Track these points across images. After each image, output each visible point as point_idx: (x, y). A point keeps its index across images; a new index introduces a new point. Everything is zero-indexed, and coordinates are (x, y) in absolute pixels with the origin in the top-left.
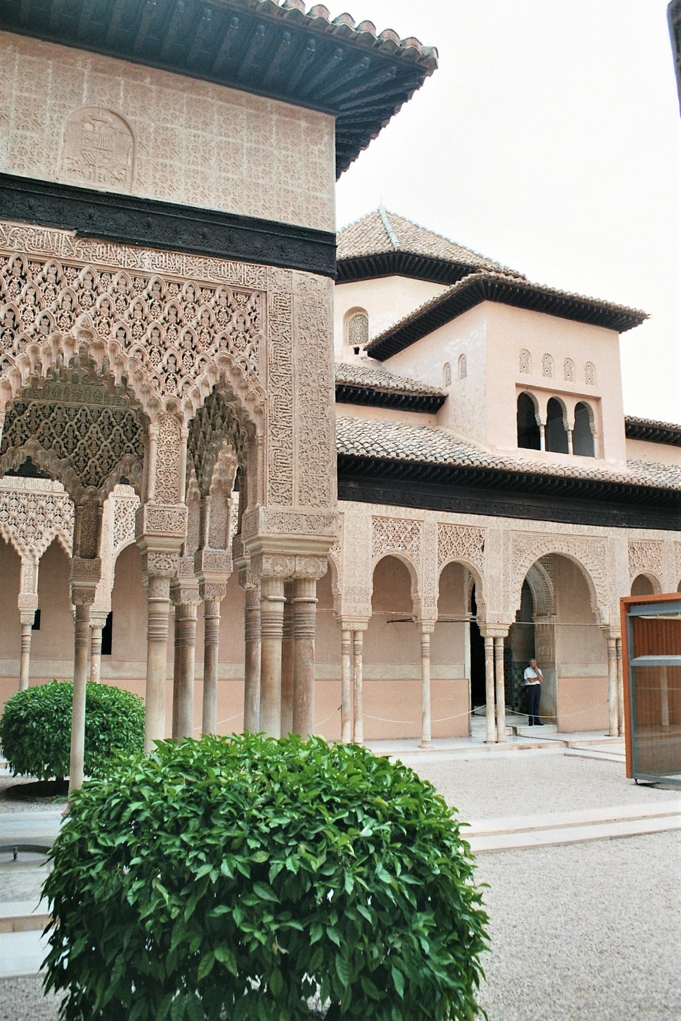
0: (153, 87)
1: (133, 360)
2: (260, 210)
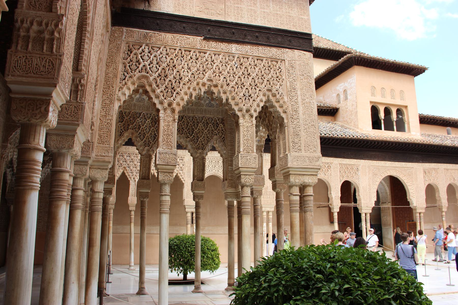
1: (231, 92)
2: (279, 25)
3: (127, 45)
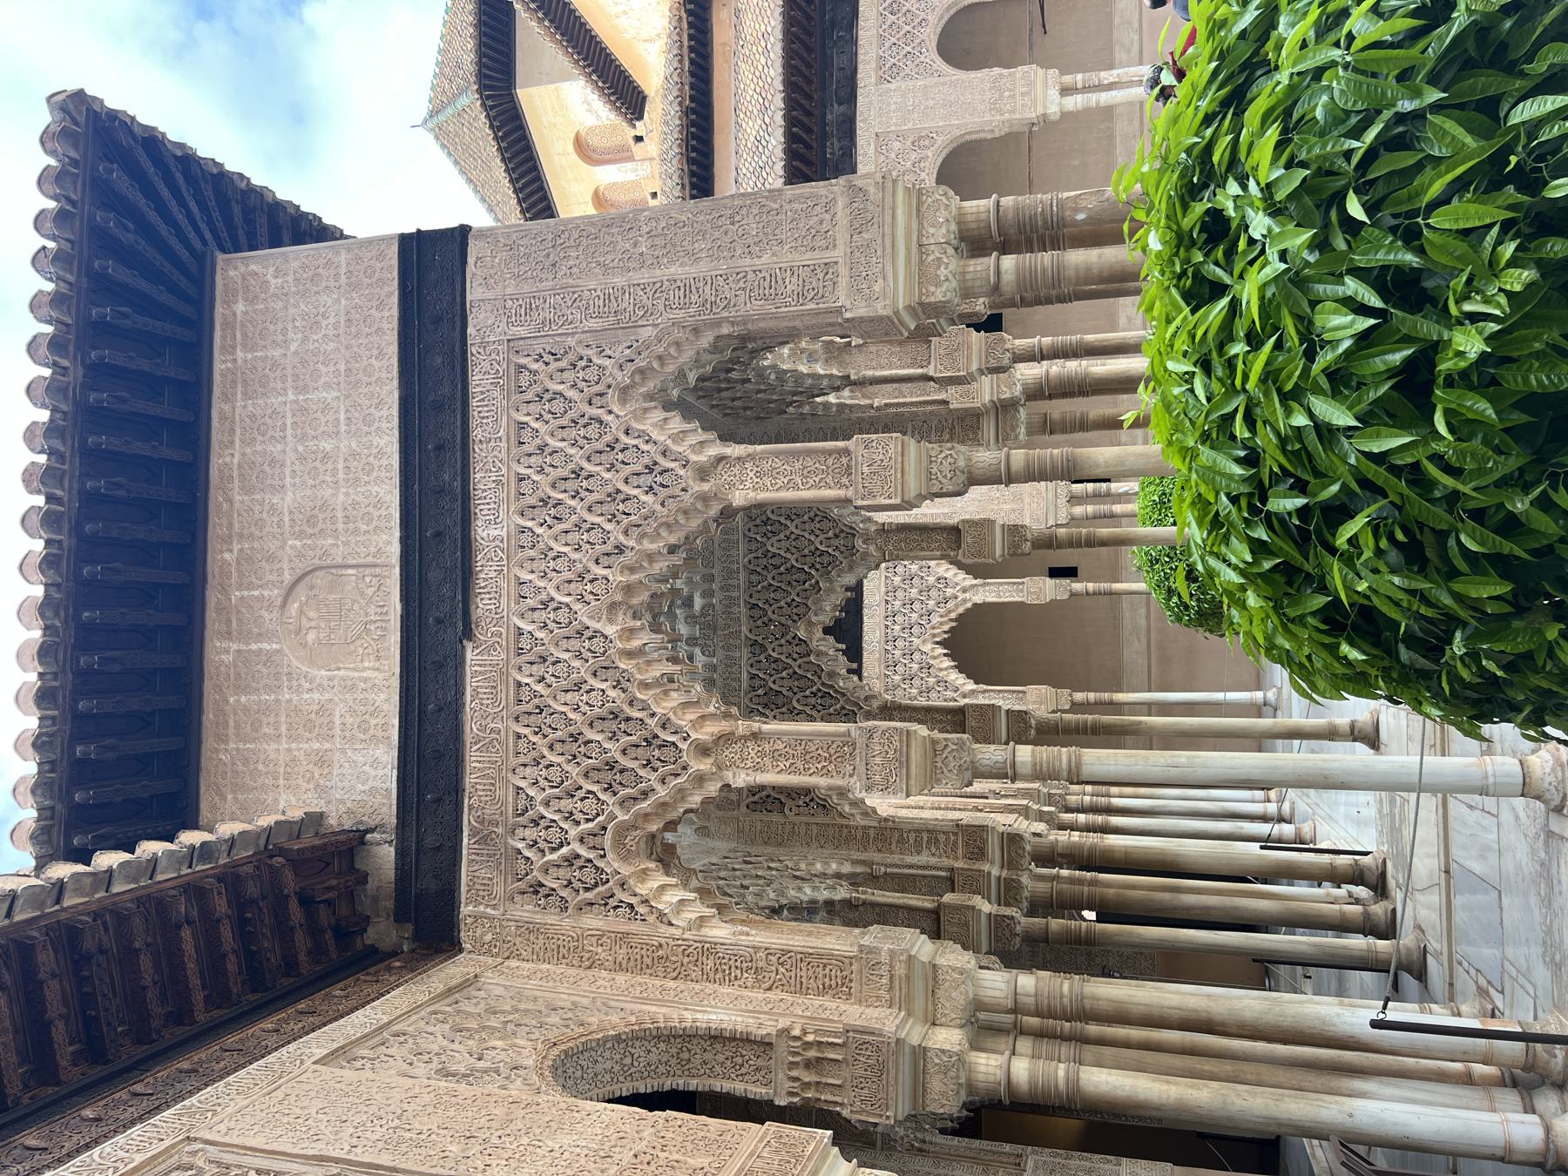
0: (236, 548)
2: (385, 363)
3: (518, 898)
